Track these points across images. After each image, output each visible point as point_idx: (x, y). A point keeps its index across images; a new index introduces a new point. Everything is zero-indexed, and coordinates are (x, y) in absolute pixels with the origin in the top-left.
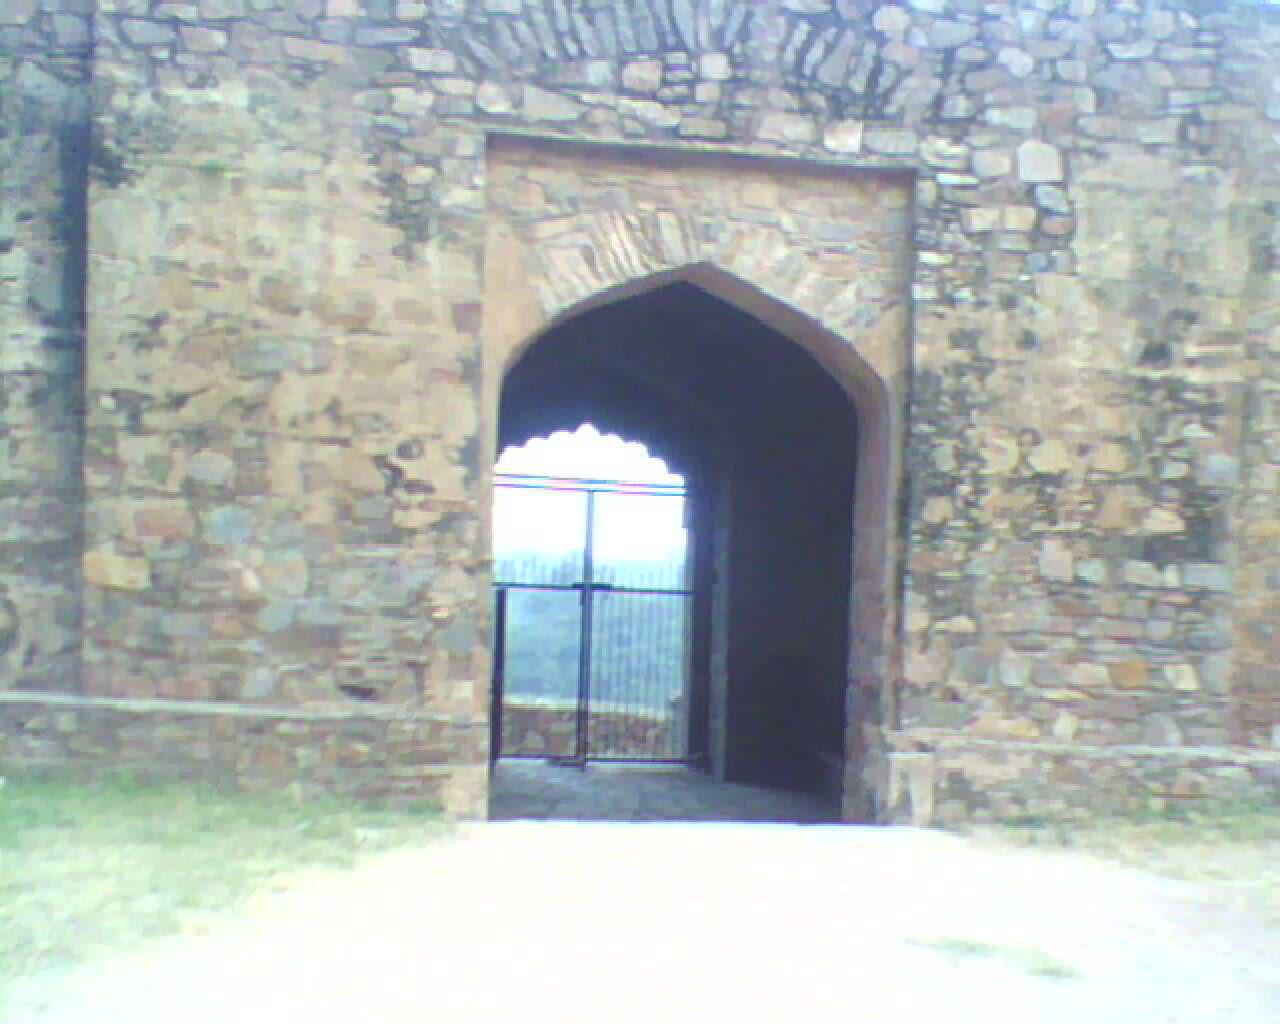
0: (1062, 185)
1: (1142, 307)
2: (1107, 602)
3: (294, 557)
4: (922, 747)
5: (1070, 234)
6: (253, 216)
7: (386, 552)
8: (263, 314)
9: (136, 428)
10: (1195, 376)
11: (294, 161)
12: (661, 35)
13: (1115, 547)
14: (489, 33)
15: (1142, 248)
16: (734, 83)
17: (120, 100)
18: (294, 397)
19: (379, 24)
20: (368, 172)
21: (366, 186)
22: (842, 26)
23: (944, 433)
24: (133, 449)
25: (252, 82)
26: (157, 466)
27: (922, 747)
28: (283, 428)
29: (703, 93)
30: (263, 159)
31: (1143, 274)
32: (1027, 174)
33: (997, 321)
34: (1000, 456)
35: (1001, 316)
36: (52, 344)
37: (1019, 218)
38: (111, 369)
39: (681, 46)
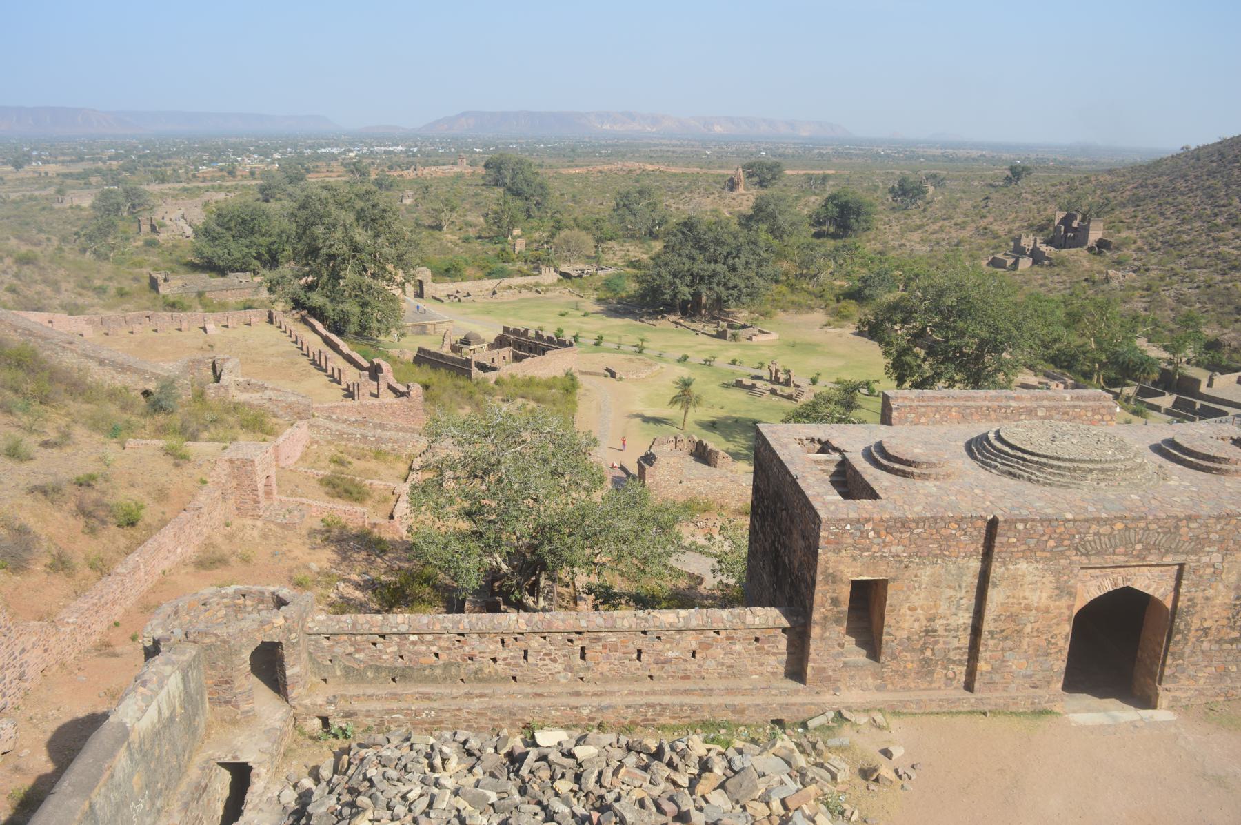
9: (992, 638)
11: (1036, 578)
14: (1084, 546)
18: (1028, 629)
20: (1052, 579)
24: (991, 642)
26: (996, 645)
30: (1029, 578)
33: (1200, 594)
34: (1196, 623)
37: (1210, 570)
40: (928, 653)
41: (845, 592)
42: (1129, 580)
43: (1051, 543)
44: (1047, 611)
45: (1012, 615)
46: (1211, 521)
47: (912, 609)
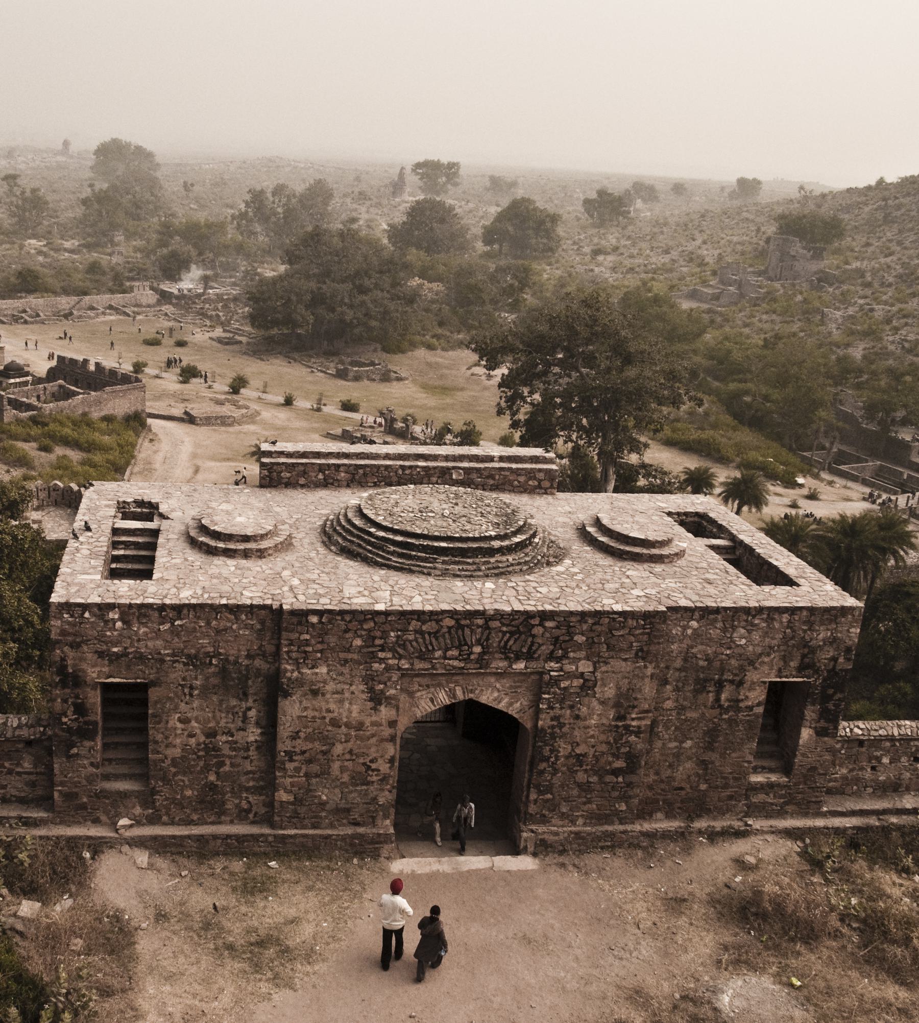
0: (593, 673)
1: (617, 705)
2: (598, 787)
3: (337, 791)
4: (532, 831)
5: (595, 686)
7: (364, 787)
8: (330, 728)
9: (291, 760)
10: (634, 723)
12: (459, 641)
16: (483, 653)
17: (288, 674)
18: (338, 749)
19: (368, 647)
20: (362, 687)
21: (363, 692)
22: (520, 633)
23: (546, 745)
24: (290, 766)
25: (328, 666)
26: (297, 770)
27: (532, 831)
28: (335, 757)
29: (472, 657)
30: (331, 686)
31: (619, 695)
32: (581, 670)
34: (564, 748)
35: (568, 712)
37: (577, 682)
38: (284, 745)
39: (466, 644)
40: (212, 778)
41: (95, 698)
42: (472, 691)
44: (360, 726)
46: (573, 619)
47: (185, 721)
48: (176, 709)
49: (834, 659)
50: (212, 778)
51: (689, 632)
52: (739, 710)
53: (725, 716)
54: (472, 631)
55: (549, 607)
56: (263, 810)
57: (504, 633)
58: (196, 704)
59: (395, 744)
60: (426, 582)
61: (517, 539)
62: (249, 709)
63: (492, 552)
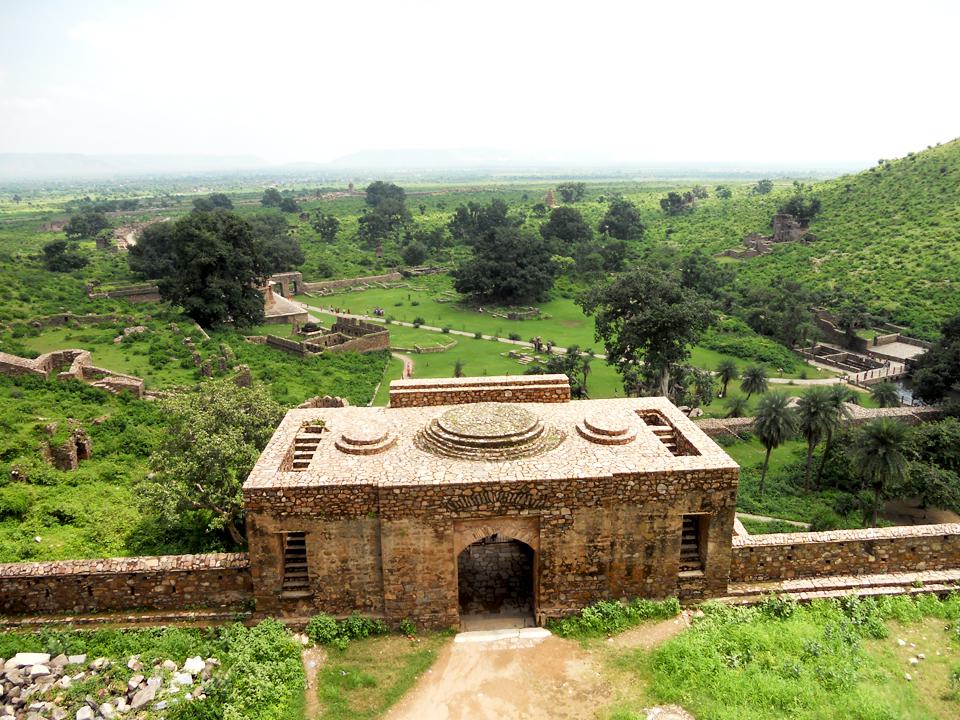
1: (588, 534)
6: (410, 539)
11: (417, 531)
13: (583, 574)
15: (588, 523)
18: (419, 567)
20: (431, 530)
24: (392, 578)
34: (558, 561)
36: (375, 559)
38: (386, 566)
40: (347, 587)
43: (425, 503)
45: (404, 557)
48: (322, 547)
49: (724, 500)
50: (347, 587)
51: (629, 488)
52: (667, 533)
53: (658, 538)
54: (494, 494)
55: (539, 478)
56: (379, 605)
57: (513, 494)
58: (333, 543)
59: (453, 562)
60: (467, 464)
61: (527, 436)
62: (365, 545)
63: (511, 444)
